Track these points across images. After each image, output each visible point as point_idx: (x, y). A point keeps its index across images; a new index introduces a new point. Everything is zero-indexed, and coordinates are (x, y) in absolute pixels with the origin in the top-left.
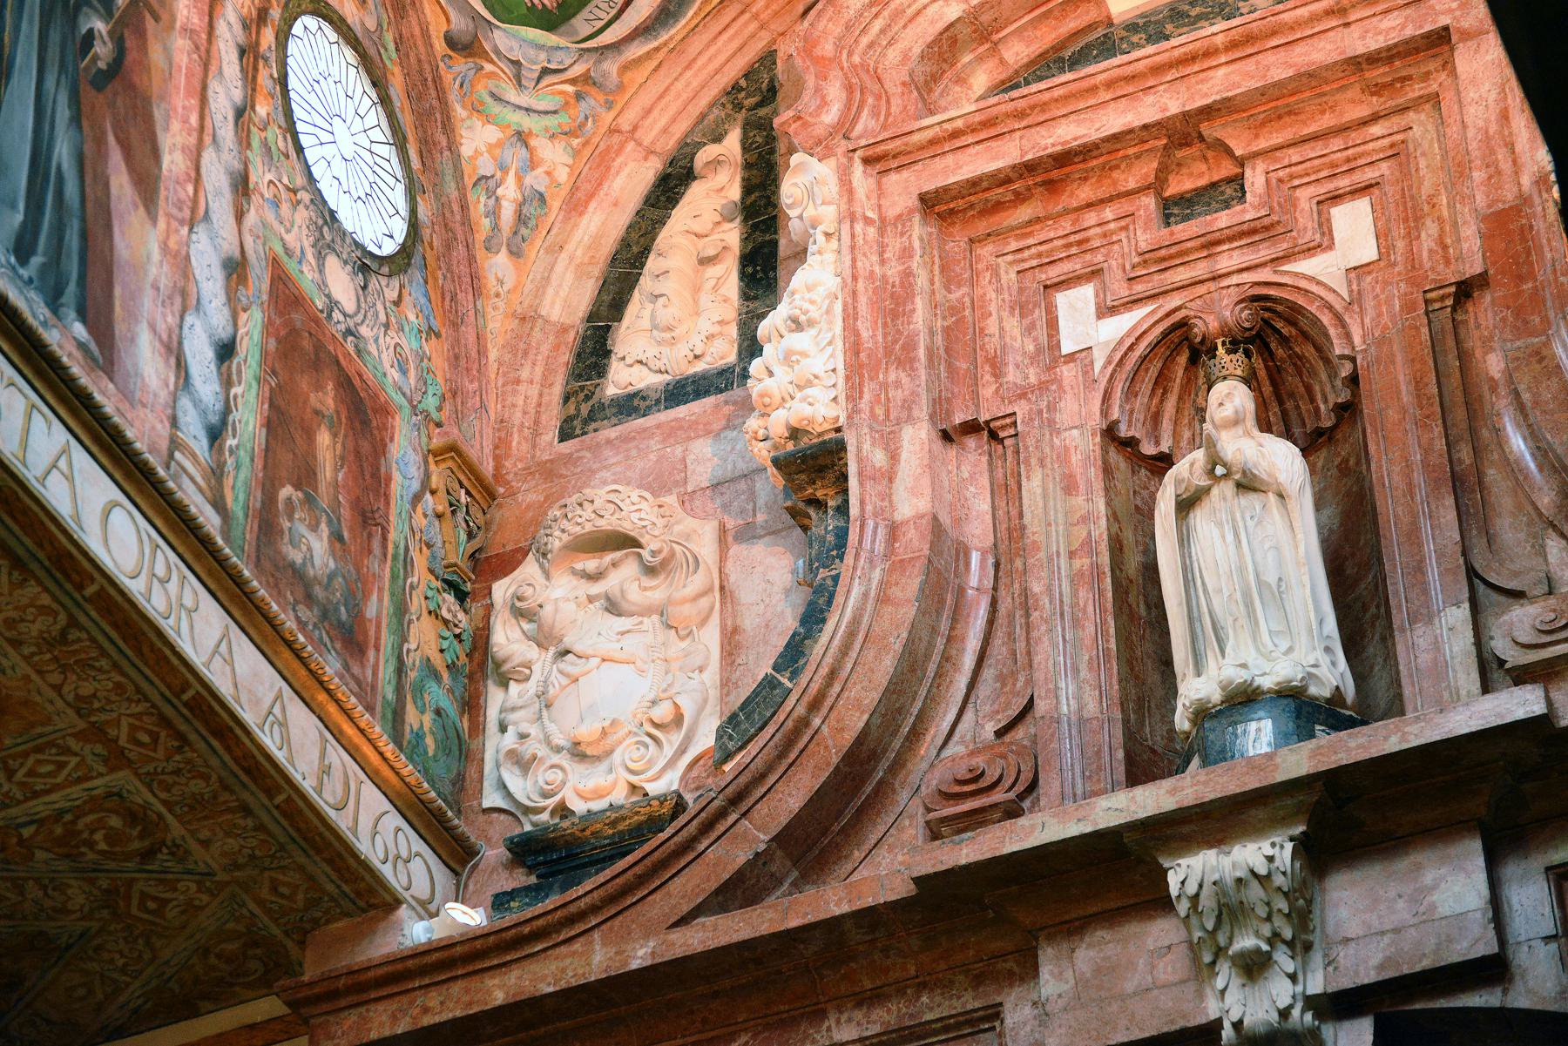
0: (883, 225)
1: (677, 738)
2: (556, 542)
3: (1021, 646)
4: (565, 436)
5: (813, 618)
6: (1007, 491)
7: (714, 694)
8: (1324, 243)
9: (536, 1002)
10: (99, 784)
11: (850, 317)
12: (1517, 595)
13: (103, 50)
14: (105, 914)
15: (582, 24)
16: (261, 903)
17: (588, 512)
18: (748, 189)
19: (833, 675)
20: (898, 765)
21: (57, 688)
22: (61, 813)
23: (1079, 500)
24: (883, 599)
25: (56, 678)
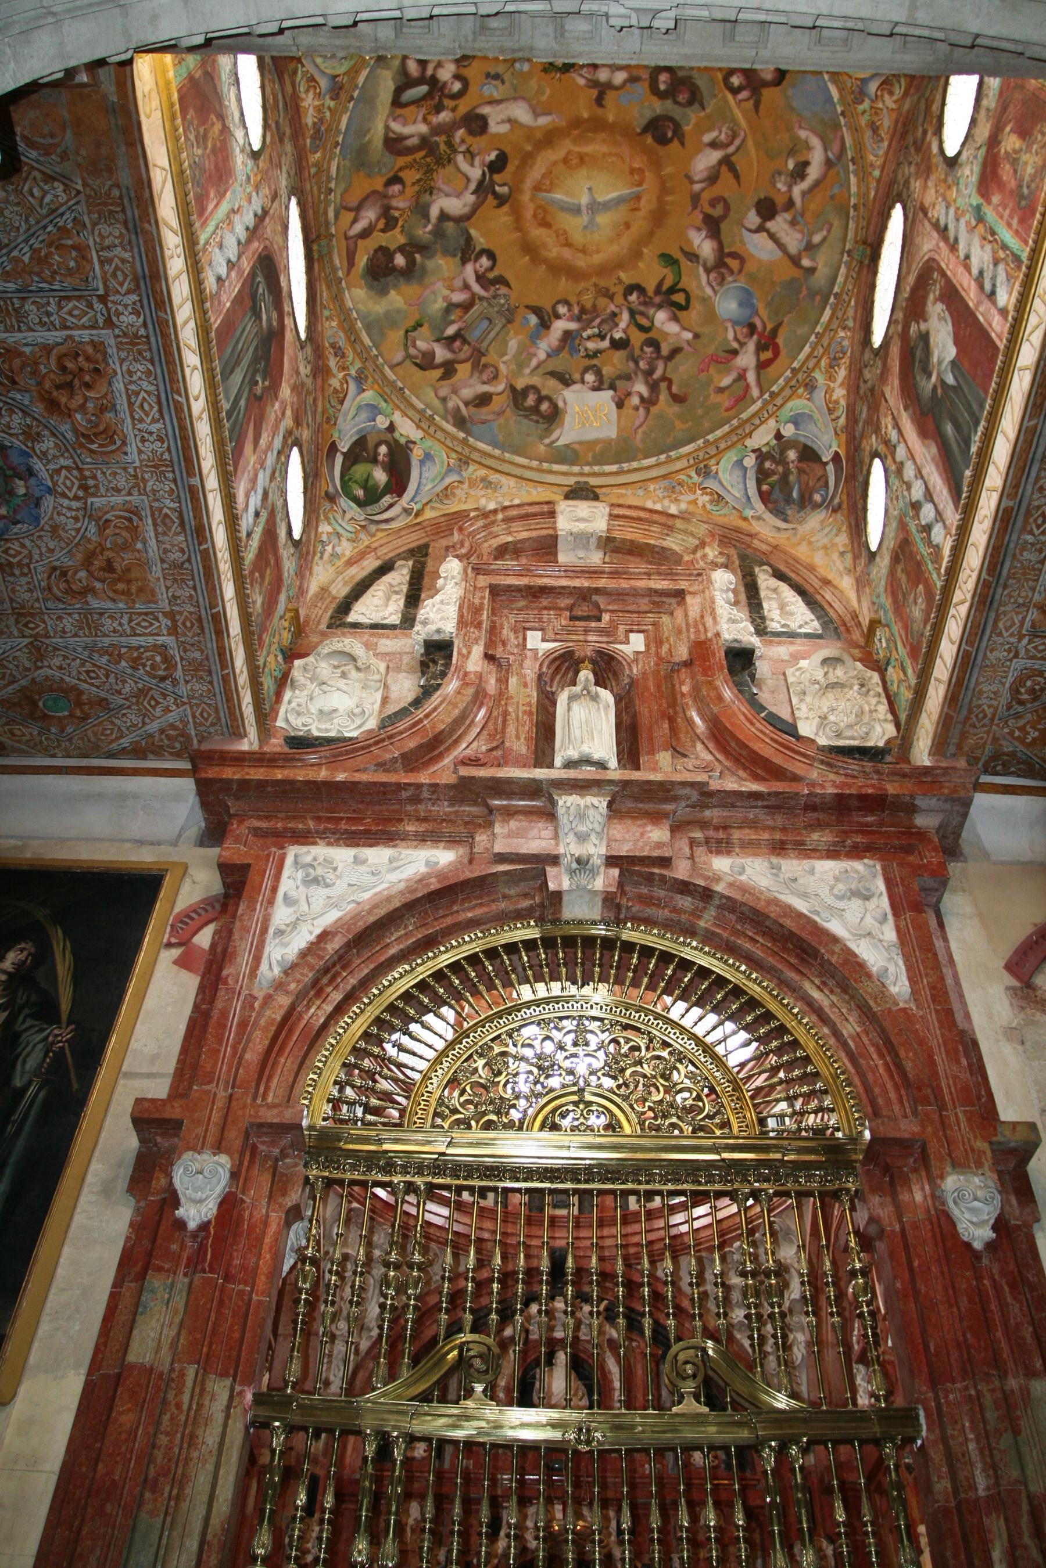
0: (475, 587)
1: (358, 722)
2: (326, 651)
3: (500, 727)
5: (417, 703)
6: (503, 681)
7: (376, 713)
8: (627, 642)
9: (293, 782)
10: (161, 640)
11: (461, 608)
12: (685, 756)
13: (258, 390)
14: (134, 700)
15: (369, 509)
16: (194, 717)
17: (341, 644)
18: (412, 578)
19: (435, 709)
20: (448, 749)
21: (167, 588)
22: (140, 647)
24: (459, 692)
25: (169, 583)
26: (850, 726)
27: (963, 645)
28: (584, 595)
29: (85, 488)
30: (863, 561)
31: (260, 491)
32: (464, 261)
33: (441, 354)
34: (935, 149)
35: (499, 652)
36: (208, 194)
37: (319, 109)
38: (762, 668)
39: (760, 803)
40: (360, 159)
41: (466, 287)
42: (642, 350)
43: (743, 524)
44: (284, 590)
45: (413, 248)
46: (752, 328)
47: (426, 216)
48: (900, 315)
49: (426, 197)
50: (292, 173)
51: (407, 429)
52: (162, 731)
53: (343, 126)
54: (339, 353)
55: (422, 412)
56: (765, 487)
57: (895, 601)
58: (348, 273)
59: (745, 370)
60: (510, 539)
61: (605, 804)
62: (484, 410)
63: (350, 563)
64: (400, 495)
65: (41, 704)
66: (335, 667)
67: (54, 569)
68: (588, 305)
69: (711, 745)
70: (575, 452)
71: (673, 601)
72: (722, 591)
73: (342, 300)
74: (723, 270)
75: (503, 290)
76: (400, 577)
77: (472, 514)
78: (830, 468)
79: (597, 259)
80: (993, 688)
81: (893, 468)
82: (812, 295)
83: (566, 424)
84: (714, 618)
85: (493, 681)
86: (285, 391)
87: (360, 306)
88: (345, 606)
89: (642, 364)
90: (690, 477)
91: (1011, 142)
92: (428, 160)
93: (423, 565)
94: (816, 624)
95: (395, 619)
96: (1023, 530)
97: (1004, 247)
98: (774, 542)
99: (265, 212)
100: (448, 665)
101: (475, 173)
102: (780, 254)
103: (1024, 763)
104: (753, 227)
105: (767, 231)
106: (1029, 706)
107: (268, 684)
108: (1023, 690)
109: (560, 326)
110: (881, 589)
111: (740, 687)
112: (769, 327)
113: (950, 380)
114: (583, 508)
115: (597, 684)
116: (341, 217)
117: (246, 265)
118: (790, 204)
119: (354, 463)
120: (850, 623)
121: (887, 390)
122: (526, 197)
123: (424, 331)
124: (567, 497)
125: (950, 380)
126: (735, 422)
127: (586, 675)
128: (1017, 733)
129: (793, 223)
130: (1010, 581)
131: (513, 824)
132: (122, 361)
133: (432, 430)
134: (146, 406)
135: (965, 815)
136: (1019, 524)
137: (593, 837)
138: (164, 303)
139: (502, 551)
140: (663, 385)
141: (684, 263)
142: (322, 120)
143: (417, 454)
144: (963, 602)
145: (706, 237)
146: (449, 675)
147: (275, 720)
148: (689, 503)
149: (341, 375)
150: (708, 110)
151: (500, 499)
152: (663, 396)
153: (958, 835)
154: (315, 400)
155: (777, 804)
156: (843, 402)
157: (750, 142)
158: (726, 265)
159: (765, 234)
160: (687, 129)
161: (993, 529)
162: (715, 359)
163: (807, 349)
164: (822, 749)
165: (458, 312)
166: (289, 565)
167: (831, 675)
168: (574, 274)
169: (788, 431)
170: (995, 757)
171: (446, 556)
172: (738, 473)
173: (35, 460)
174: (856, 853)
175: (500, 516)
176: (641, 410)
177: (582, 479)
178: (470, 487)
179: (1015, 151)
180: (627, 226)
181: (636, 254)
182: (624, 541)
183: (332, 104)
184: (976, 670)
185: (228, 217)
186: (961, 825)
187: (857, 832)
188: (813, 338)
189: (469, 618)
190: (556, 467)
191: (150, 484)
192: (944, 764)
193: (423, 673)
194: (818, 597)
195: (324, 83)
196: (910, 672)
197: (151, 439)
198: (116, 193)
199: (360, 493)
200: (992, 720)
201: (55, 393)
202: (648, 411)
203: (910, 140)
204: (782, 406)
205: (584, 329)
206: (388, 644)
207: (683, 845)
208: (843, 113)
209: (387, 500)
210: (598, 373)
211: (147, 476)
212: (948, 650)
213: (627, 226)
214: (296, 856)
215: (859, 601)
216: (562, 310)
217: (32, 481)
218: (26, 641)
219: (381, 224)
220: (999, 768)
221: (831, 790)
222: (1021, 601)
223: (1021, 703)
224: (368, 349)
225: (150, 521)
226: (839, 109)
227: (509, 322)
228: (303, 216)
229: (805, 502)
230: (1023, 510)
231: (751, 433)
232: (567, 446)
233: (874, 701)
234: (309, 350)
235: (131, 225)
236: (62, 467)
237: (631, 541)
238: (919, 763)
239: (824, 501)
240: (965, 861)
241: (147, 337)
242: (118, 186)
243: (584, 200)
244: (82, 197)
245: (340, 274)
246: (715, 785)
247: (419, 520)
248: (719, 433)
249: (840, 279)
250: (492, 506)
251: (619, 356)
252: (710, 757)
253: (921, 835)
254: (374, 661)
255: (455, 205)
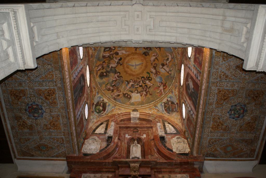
0: (117, 127)
2: (91, 138)
4: (92, 134)
5: (106, 147)
6: (121, 143)
8: (143, 136)
11: (114, 130)
12: (153, 156)
13: (80, 95)
15: (99, 114)
16: (67, 150)
18: (106, 125)
19: (109, 149)
20: (111, 156)
21: (63, 128)
23: (126, 145)
24: (113, 145)
26: (182, 150)
27: (199, 135)
28: (135, 128)
29: (50, 111)
30: (183, 120)
31: (80, 111)
32: (115, 74)
33: (111, 88)
34: (187, 56)
35: (121, 138)
36: (73, 66)
37: (92, 52)
38: (167, 140)
39: (166, 164)
40: (99, 59)
41: (116, 78)
42: (144, 87)
43: (163, 115)
44: (84, 128)
45: (107, 72)
46: (162, 83)
47: (109, 67)
48: (185, 81)
49: (109, 64)
50: (88, 61)
51: (106, 100)
52: (61, 153)
53: (96, 54)
54: (95, 88)
55: (108, 98)
56: (166, 109)
57: (188, 127)
58: (97, 76)
59: (161, 90)
60: (123, 118)
61: (139, 165)
62: (119, 97)
63: (96, 123)
64: (104, 111)
65: (41, 148)
66: (92, 141)
67: (45, 125)
68: (135, 80)
69: (158, 154)
70: (134, 104)
71: (151, 128)
72: (159, 126)
73: (95, 80)
74: (157, 74)
75: (122, 78)
76: (104, 125)
77: (116, 114)
78: (176, 105)
79: (137, 73)
80: (205, 142)
81: (186, 105)
82: (171, 78)
83: (132, 99)
84: (158, 131)
85: (119, 143)
86: (85, 95)
87: (99, 81)
88: (95, 130)
89: (144, 89)
90: (153, 107)
91: (198, 56)
92: (109, 59)
93: (108, 123)
94: (175, 131)
95: (103, 132)
96: (207, 115)
97: (198, 71)
98: (168, 118)
99: (83, 68)
100: (111, 141)
101: (117, 61)
102: (165, 71)
103: (213, 155)
104: (161, 68)
105: (163, 68)
106: (212, 145)
107: (80, 144)
108: (210, 142)
109: (131, 83)
110: (186, 125)
111: (162, 143)
112: (165, 83)
113: (193, 91)
114: (135, 113)
115: (138, 143)
116: (95, 68)
117: (79, 76)
118: (167, 64)
119: (97, 106)
120: (181, 131)
121: (184, 92)
122: (125, 64)
123: (109, 84)
124: (133, 111)
125: (193, 91)
126: (160, 98)
127: (136, 142)
128: (211, 150)
129: (167, 67)
130: (206, 124)
131: (123, 169)
132: (58, 91)
133: (110, 100)
134: (61, 98)
135: (203, 165)
136: (206, 114)
137: (137, 171)
138: (65, 83)
139: (121, 121)
140: (148, 92)
141: (151, 73)
142: (92, 54)
143: (107, 104)
144: (198, 127)
145: (154, 69)
146: (112, 142)
147: (81, 150)
148: (153, 111)
149: (95, 92)
150: (153, 51)
151: (121, 112)
152: (148, 94)
153: (202, 169)
154: (90, 96)
155: (170, 164)
156: (177, 94)
157: (160, 55)
158: (157, 73)
159: (163, 69)
160: (150, 54)
161: (202, 115)
162: (156, 88)
163: (171, 86)
164: (177, 154)
165: (114, 81)
166: (85, 123)
167: (178, 140)
168: (133, 75)
169: (169, 99)
170: (207, 154)
171: (112, 122)
172: (161, 106)
173: (43, 107)
174: (184, 173)
175: (121, 115)
176: (145, 97)
177: (135, 108)
178: (116, 110)
179: (198, 57)
180: (141, 68)
181: (143, 72)
182: (142, 118)
183: (94, 52)
184: (202, 139)
185: (76, 69)
186: (203, 167)
187: (184, 169)
188: (172, 84)
189: (115, 132)
190: (131, 106)
191: (61, 111)
192: (198, 156)
193: (107, 142)
194: (176, 127)
195: (93, 49)
196: (191, 139)
197: (62, 103)
198: (58, 66)
199: (98, 111)
200: (206, 147)
201: (47, 97)
202: (146, 96)
203: (184, 55)
204: (168, 95)
205: (135, 84)
206: (101, 137)
207: (153, 172)
208: (173, 51)
209: (102, 112)
210: (137, 91)
211: (61, 109)
212: (197, 135)
213: (141, 68)
214: (84, 175)
215: (183, 127)
216: (131, 81)
217: (42, 110)
218: (39, 137)
219: (102, 69)
220: (208, 156)
221: (179, 161)
222: (208, 127)
223: (211, 144)
224: (99, 88)
225: (61, 117)
226: (173, 50)
227: (123, 83)
228: (89, 68)
229: (172, 111)
230: (206, 112)
231: (163, 100)
232: (133, 103)
233: (186, 145)
234: (90, 88)
235: (60, 71)
236: (47, 108)
237: (143, 118)
238: (194, 156)
239: (176, 110)
240: (204, 173)
241: (62, 88)
242: (59, 65)
243: (134, 64)
244: (53, 67)
245: (95, 76)
246: (158, 161)
247: (108, 115)
248: (158, 100)
249: (175, 75)
250: (120, 113)
251: (141, 88)
252: (157, 156)
253: (196, 169)
254: (99, 140)
255: (114, 66)
